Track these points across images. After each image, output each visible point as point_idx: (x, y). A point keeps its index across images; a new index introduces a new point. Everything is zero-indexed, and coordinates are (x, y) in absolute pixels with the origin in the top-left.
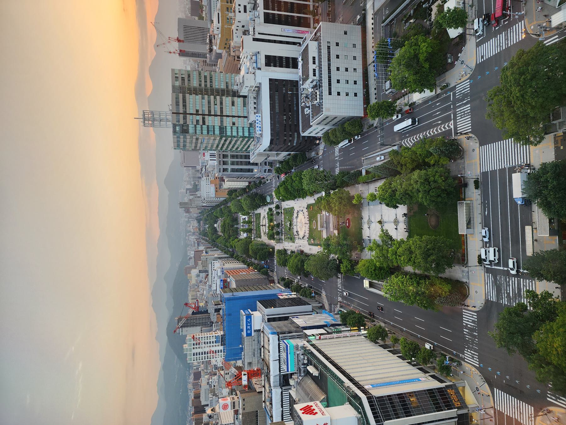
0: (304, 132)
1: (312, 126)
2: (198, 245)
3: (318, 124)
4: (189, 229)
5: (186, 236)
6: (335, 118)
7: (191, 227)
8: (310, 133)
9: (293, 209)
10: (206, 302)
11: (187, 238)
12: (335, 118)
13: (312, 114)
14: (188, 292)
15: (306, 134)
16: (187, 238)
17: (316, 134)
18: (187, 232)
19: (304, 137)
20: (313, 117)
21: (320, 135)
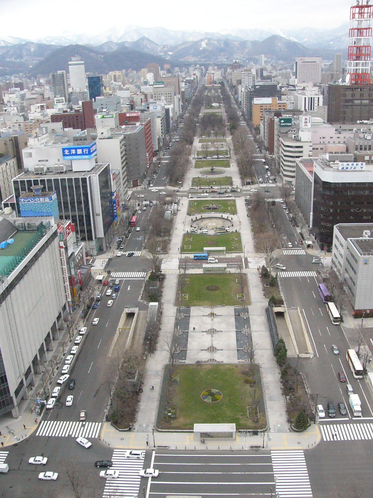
0: (341, 229)
1: (346, 240)
2: (187, 81)
3: (348, 248)
4: (210, 68)
5: (201, 65)
6: (355, 273)
7: (213, 72)
8: (336, 237)
9: (234, 212)
10: (111, 95)
11: (198, 66)
12: (355, 273)
13: (362, 240)
14: (124, 71)
15: (336, 231)
16: (198, 66)
17: (336, 246)
18: (206, 66)
19: (332, 229)
20: (357, 241)
21: (334, 250)
